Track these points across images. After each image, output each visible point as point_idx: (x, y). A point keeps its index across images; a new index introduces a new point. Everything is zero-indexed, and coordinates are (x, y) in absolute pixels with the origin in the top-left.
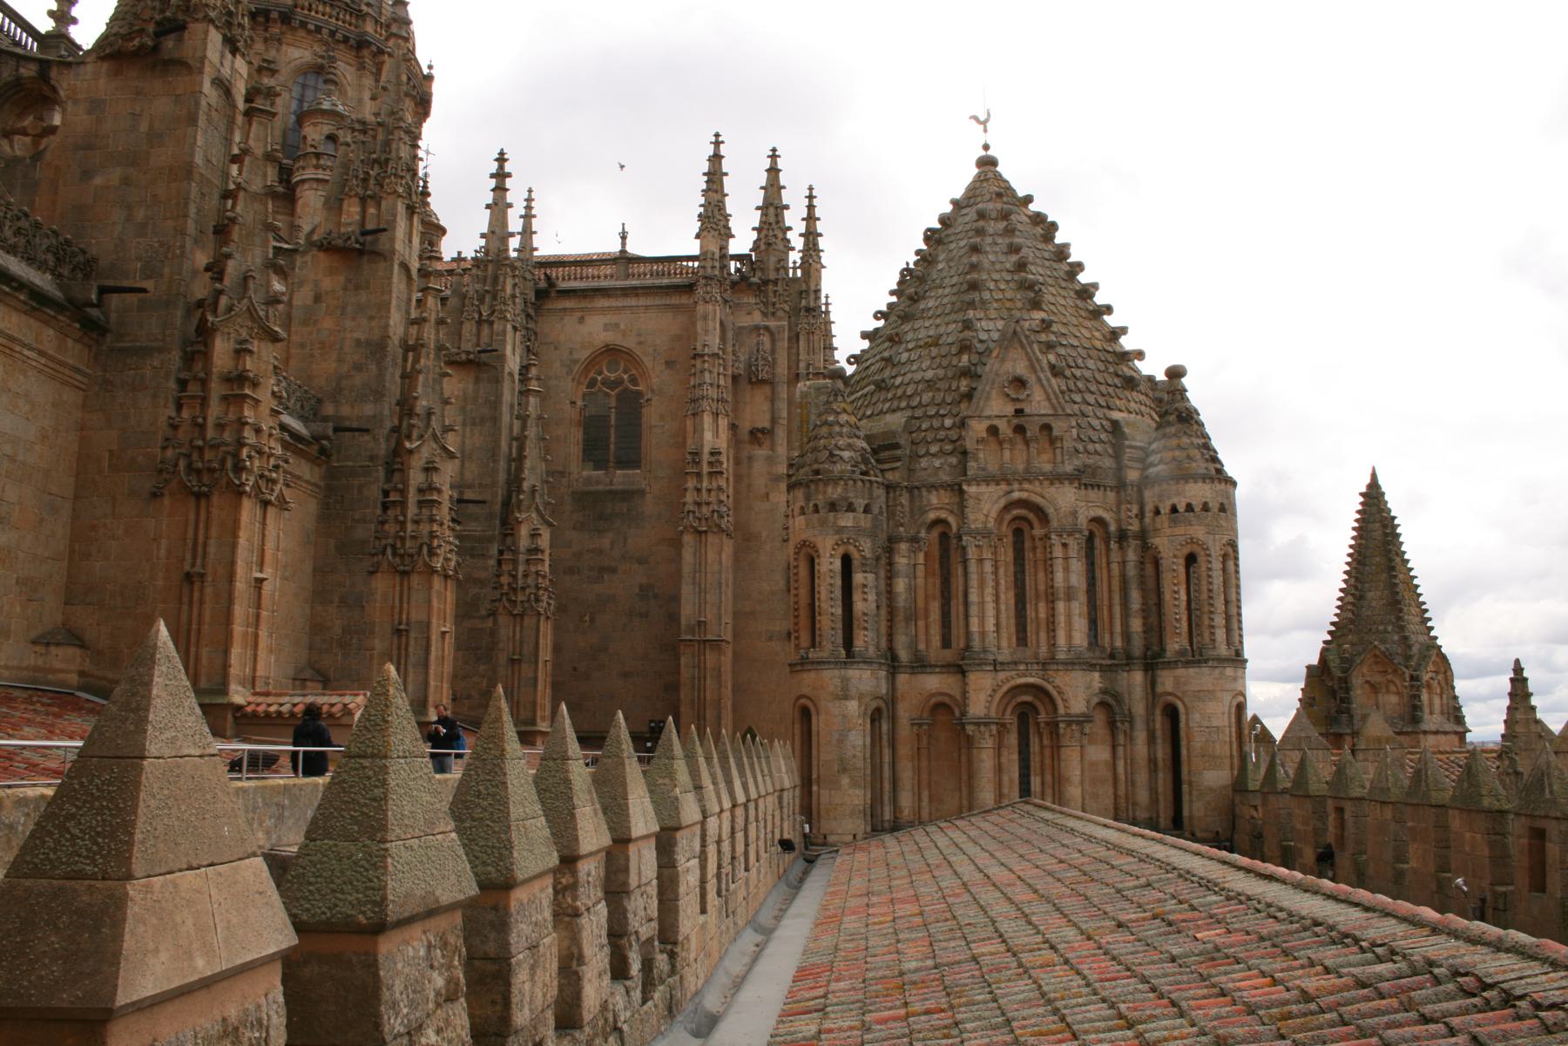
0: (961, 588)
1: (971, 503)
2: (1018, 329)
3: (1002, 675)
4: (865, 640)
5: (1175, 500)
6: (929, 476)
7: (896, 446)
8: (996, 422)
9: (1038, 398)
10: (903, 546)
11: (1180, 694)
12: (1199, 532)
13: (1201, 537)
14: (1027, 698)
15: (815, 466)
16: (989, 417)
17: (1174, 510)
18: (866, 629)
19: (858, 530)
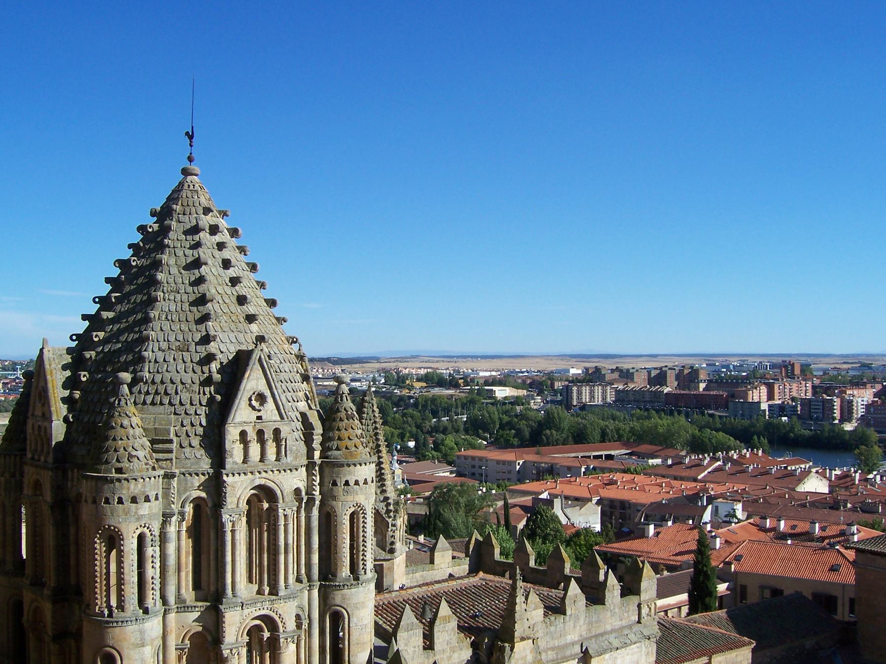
0: (212, 549)
1: (229, 490)
2: (263, 357)
3: (246, 611)
4: (153, 599)
5: (348, 478)
6: (192, 464)
7: (171, 441)
8: (247, 428)
9: (271, 408)
10: (174, 519)
11: (345, 607)
12: (361, 499)
13: (362, 503)
14: (258, 622)
15: (119, 465)
16: (241, 424)
17: (347, 483)
18: (153, 589)
19: (151, 516)
